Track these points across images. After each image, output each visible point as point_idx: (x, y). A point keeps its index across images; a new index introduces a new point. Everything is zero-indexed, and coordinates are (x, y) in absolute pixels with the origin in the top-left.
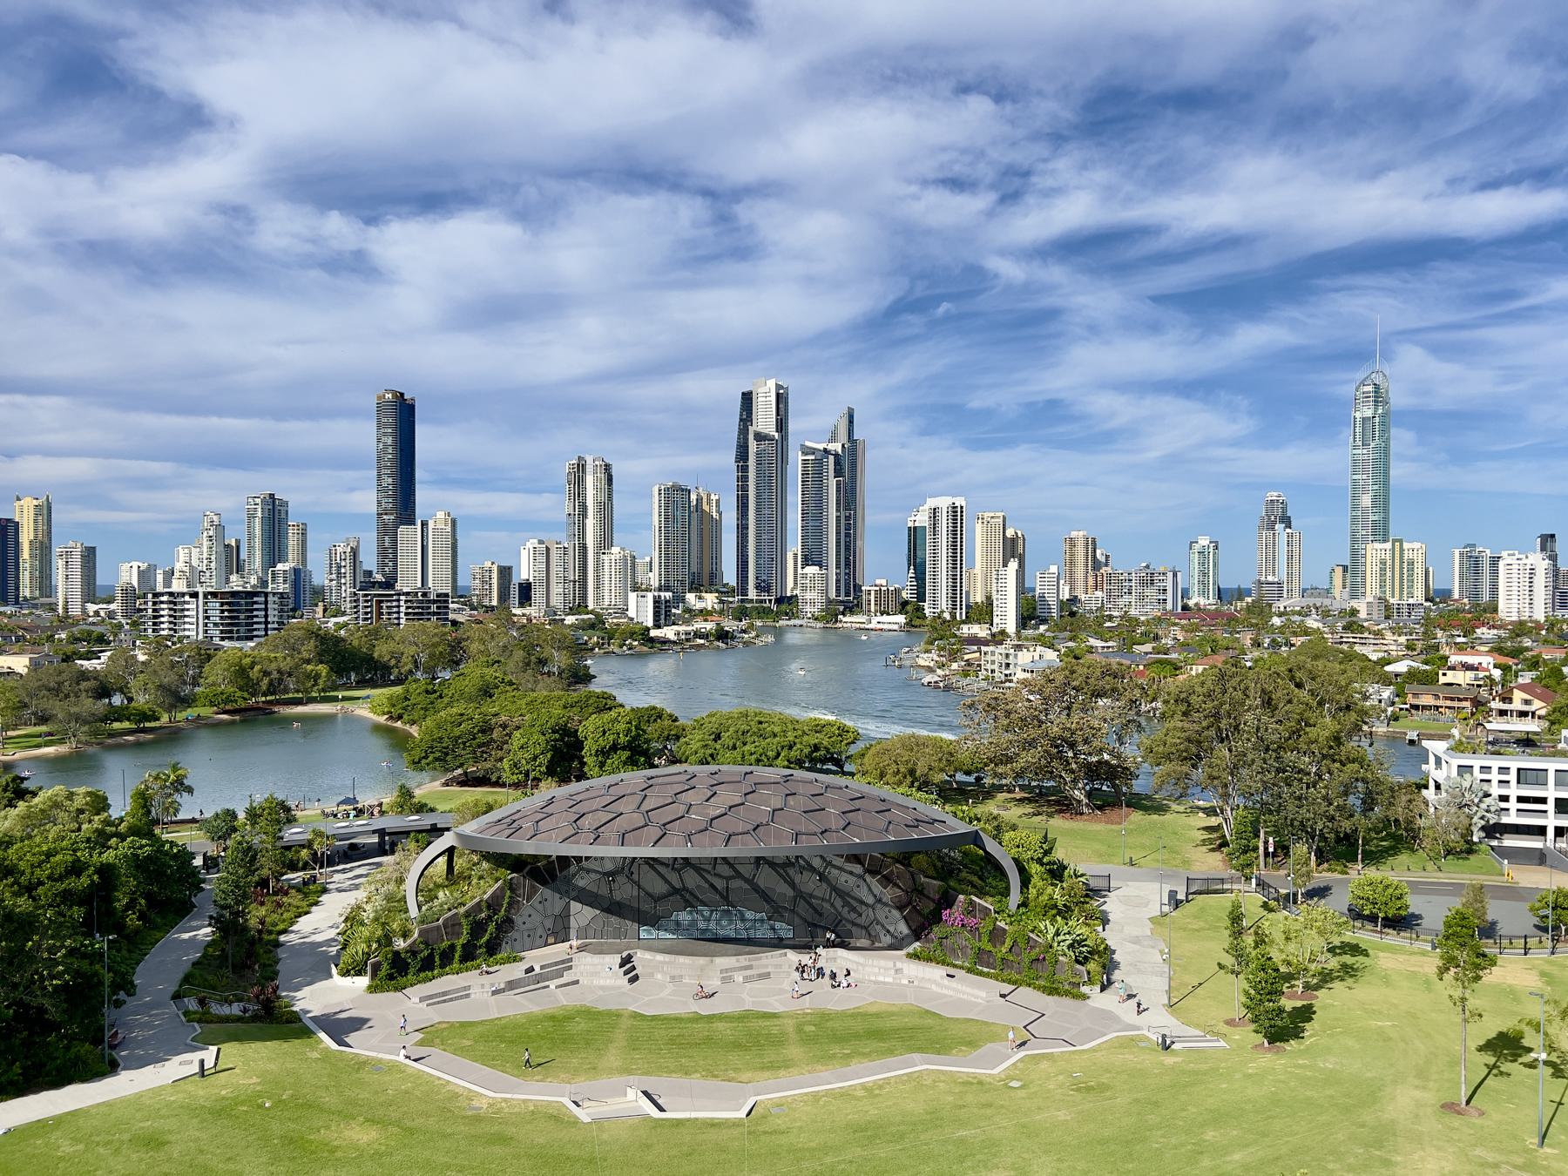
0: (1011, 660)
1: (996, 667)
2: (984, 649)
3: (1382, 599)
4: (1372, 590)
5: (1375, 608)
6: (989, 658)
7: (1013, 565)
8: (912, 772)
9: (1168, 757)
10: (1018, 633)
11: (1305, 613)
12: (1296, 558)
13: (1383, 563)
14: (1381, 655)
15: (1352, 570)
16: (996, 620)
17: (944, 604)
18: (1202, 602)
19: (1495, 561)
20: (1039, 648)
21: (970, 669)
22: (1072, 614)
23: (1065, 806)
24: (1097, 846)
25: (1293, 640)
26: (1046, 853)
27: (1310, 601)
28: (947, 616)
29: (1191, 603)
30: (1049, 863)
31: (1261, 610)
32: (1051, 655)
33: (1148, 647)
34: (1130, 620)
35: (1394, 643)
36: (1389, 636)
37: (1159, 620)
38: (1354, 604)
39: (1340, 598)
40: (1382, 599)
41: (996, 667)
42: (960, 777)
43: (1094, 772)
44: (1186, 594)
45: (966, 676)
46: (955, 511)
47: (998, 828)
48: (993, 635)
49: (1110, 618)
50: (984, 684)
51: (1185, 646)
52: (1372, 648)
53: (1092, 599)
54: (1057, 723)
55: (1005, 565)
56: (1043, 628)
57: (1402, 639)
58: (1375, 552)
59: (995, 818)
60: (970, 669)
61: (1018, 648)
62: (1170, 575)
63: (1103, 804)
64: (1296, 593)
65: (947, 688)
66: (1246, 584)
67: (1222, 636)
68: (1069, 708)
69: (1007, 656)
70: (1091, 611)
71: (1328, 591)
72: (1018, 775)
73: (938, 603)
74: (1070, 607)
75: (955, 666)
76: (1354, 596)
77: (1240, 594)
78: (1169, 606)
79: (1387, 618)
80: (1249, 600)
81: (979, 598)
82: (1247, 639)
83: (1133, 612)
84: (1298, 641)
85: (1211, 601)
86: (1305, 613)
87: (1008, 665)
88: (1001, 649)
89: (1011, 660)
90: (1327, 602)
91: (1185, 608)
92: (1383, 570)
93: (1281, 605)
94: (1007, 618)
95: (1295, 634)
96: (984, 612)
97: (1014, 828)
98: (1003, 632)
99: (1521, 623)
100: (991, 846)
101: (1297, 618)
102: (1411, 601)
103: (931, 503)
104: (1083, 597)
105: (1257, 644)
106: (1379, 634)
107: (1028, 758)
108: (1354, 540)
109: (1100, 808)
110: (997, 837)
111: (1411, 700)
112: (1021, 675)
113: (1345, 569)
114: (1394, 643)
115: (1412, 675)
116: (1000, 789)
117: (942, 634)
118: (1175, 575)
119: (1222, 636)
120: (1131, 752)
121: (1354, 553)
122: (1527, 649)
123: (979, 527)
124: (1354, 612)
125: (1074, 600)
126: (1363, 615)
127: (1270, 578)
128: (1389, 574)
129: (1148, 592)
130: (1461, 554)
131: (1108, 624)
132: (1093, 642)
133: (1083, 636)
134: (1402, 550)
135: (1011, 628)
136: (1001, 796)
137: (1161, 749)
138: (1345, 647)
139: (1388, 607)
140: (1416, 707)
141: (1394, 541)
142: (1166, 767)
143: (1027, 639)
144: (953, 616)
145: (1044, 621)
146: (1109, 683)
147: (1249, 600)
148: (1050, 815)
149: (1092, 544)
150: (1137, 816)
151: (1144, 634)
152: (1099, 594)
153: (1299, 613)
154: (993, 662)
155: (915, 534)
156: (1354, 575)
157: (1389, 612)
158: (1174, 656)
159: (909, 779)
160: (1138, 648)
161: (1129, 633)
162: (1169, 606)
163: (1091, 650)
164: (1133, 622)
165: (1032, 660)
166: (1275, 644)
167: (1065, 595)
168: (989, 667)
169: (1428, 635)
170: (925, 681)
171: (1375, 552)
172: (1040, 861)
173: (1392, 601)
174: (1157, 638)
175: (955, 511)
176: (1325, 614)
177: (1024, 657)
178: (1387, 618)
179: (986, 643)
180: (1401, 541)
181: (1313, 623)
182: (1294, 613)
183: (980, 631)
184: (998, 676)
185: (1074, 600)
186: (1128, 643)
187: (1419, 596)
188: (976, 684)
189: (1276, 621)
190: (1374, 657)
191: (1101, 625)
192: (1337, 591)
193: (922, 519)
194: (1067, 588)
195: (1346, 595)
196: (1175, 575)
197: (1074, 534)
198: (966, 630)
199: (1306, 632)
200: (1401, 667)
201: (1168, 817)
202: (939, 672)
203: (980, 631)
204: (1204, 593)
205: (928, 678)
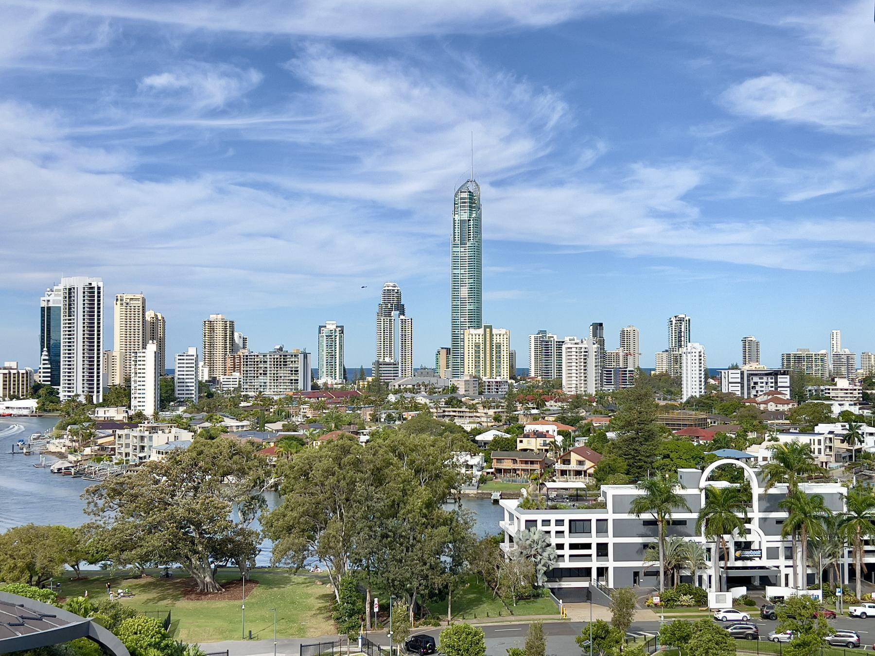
0: (146, 443)
1: (130, 450)
2: (119, 432)
3: (477, 378)
4: (469, 369)
5: (471, 386)
6: (123, 441)
7: (152, 347)
8: (30, 567)
9: (289, 529)
10: (156, 415)
11: (415, 390)
12: (408, 342)
13: (477, 346)
14: (474, 426)
15: (453, 352)
16: (134, 403)
17: (79, 387)
18: (330, 381)
19: (560, 344)
20: (174, 430)
21: (104, 453)
22: (210, 395)
23: (189, 587)
24: (219, 623)
25: (405, 415)
26: (164, 637)
27: (420, 380)
28: (82, 399)
29: (320, 382)
30: (167, 646)
31: (379, 389)
32: (186, 436)
33: (278, 425)
34: (264, 399)
35: (486, 415)
36: (481, 410)
37: (290, 399)
38: (455, 382)
39: (445, 377)
40: (477, 378)
41: (130, 450)
42: (84, 566)
43: (218, 550)
44: (315, 374)
45: (99, 460)
46: (92, 293)
47: (116, 618)
48: (130, 418)
49: (247, 398)
50: (116, 468)
51: (311, 422)
52: (468, 420)
53: (230, 380)
54: (183, 502)
55: (144, 347)
56: (181, 409)
57: (491, 412)
58: (472, 336)
59: (113, 607)
60: (104, 453)
61: (153, 430)
62: (301, 357)
63: (229, 584)
64: (409, 373)
65: (78, 474)
66: (368, 365)
67: (346, 413)
68: (196, 489)
69: (142, 438)
70: (228, 392)
71: (434, 371)
72: (144, 558)
73: (73, 386)
74: (207, 389)
75: (88, 451)
76: (455, 375)
77: (362, 373)
78: (300, 386)
79: (481, 393)
80: (370, 379)
81: (118, 380)
82: (366, 414)
83: (268, 393)
84: (409, 415)
85: (338, 380)
86: (415, 390)
87: (143, 448)
88: (136, 432)
89: (146, 443)
90: (433, 380)
91: (315, 387)
92: (477, 352)
93: (395, 384)
94: (146, 399)
95: (407, 409)
96: (121, 395)
97: (132, 614)
98: (140, 416)
99: (578, 397)
100: (105, 637)
101: (409, 395)
102: (498, 379)
103: (66, 282)
104: (221, 378)
105: (375, 419)
106: (473, 408)
107: (155, 541)
108: (454, 327)
109: (223, 586)
110: (113, 626)
111: (495, 464)
112: (155, 457)
113: (448, 351)
114: (486, 415)
115: (497, 443)
116: (126, 576)
117: (76, 418)
118: (305, 356)
119: (346, 413)
120: (256, 526)
121: (455, 338)
122: (583, 418)
123: (117, 309)
124: (454, 389)
125: (213, 381)
126: (462, 391)
127: (387, 360)
128: (482, 355)
129: (281, 373)
130: (536, 339)
131: (243, 404)
132: (229, 422)
133: (218, 415)
134: (491, 335)
135: (149, 410)
136: (125, 583)
137: (281, 522)
138: (447, 420)
139: (481, 384)
140: (499, 471)
141: (486, 327)
142: (287, 541)
143: (164, 420)
144: (89, 399)
145: (181, 403)
146: (240, 461)
147: (370, 379)
148: (176, 598)
149: (230, 327)
150: (258, 591)
151: (279, 412)
152: (237, 375)
153: (412, 391)
154: (127, 446)
155: (48, 315)
156: (455, 357)
157: (481, 387)
158: (301, 432)
159: (27, 576)
160: (270, 427)
161: (262, 412)
162: (300, 386)
163: (225, 430)
164: (267, 402)
165: (167, 441)
166: (390, 418)
167: (204, 375)
168: (123, 450)
169: (511, 408)
170: (55, 467)
171: (472, 336)
172: (157, 646)
173: (484, 379)
174: (288, 416)
175: (92, 293)
176: (431, 392)
177: (160, 440)
178: (481, 393)
179: (121, 425)
180: (490, 327)
181: (422, 399)
182: (406, 390)
183: (116, 414)
184: (133, 459)
185: (213, 381)
186: (261, 422)
187: (505, 374)
188: (108, 469)
189: (392, 398)
190: (468, 428)
191: (236, 405)
192: (443, 372)
193: (56, 300)
194: (206, 370)
195: (449, 375)
196: (305, 356)
197: (212, 317)
198: (102, 414)
199: (416, 407)
200: (488, 436)
201: (289, 587)
202: (71, 458)
203: (116, 414)
204: (331, 374)
205: (58, 464)
